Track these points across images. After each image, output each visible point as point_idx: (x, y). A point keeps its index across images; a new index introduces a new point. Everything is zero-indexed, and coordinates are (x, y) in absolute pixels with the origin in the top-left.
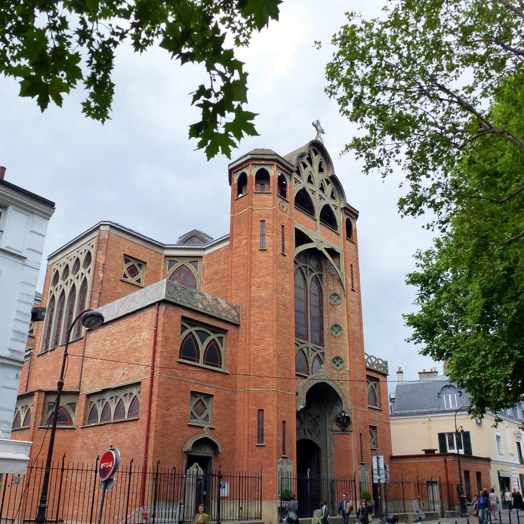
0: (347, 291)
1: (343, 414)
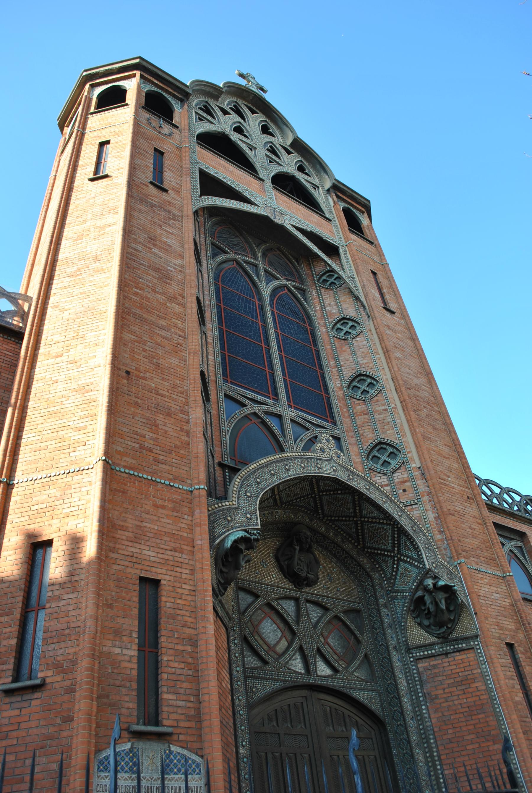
0: (370, 306)
1: (429, 582)
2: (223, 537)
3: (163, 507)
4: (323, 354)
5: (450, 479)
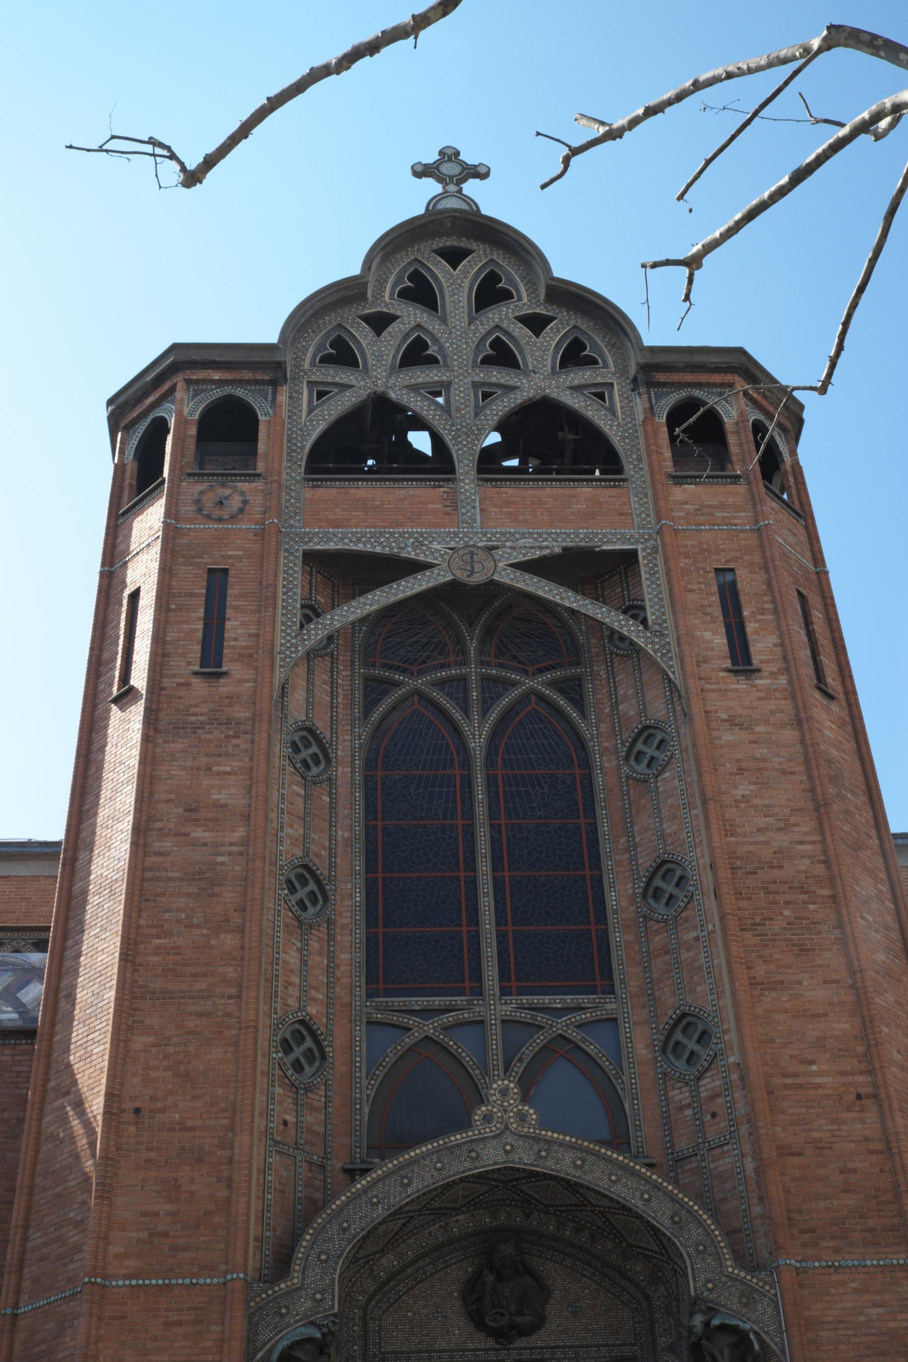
2: (269, 1346)
3: (179, 1323)
4: (604, 828)
5: (814, 1068)
